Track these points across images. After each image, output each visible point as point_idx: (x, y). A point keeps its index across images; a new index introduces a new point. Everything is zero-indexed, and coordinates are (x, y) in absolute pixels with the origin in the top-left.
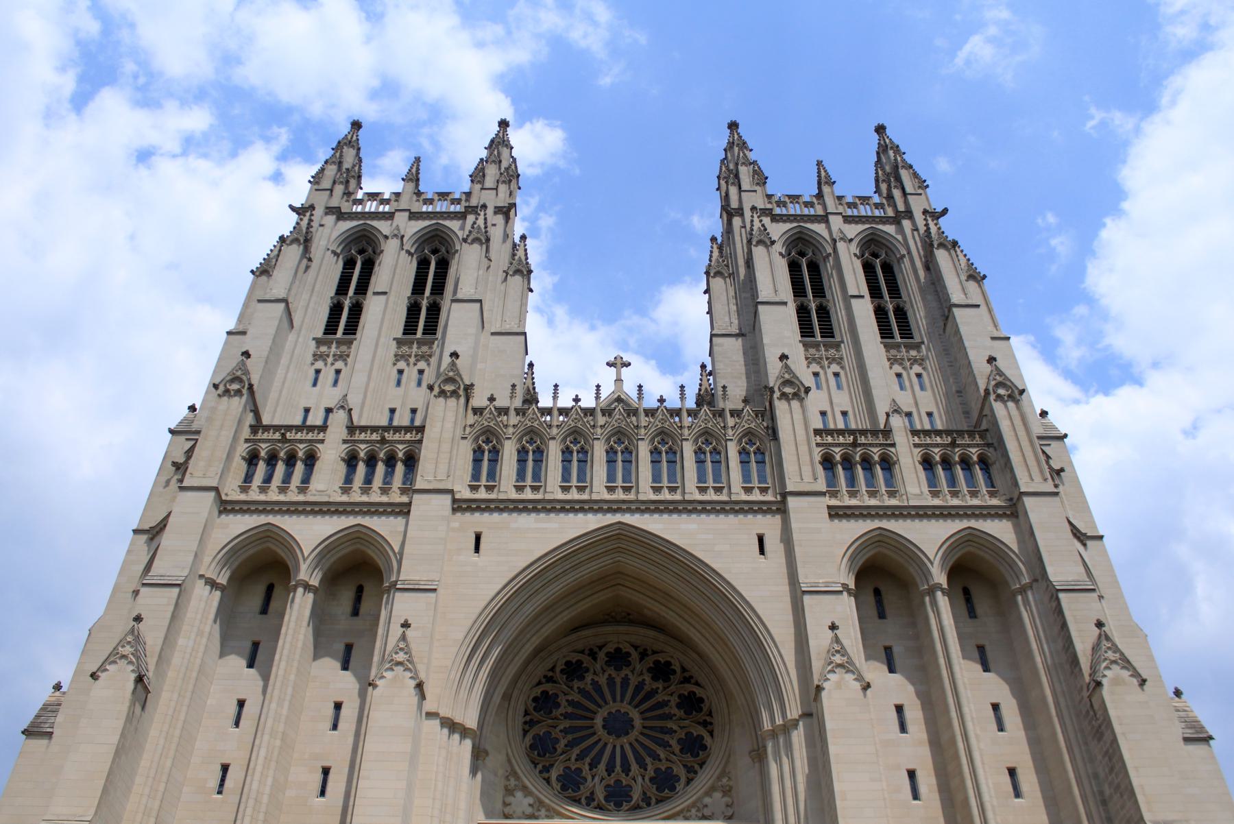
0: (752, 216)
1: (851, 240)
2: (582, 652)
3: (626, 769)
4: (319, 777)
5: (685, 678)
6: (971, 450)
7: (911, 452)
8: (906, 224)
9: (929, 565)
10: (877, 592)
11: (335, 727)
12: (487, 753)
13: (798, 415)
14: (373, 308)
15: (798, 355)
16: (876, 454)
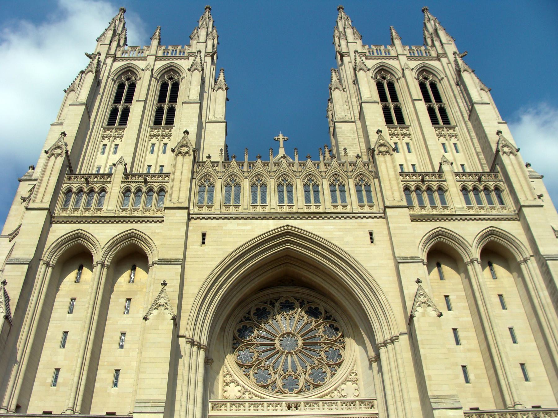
0: (355, 56)
1: (412, 69)
3: (295, 369)
5: (327, 316)
6: (490, 183)
7: (456, 185)
8: (444, 60)
9: (470, 247)
11: (121, 347)
12: (212, 360)
13: (389, 164)
14: (136, 109)
15: (386, 131)
16: (435, 185)
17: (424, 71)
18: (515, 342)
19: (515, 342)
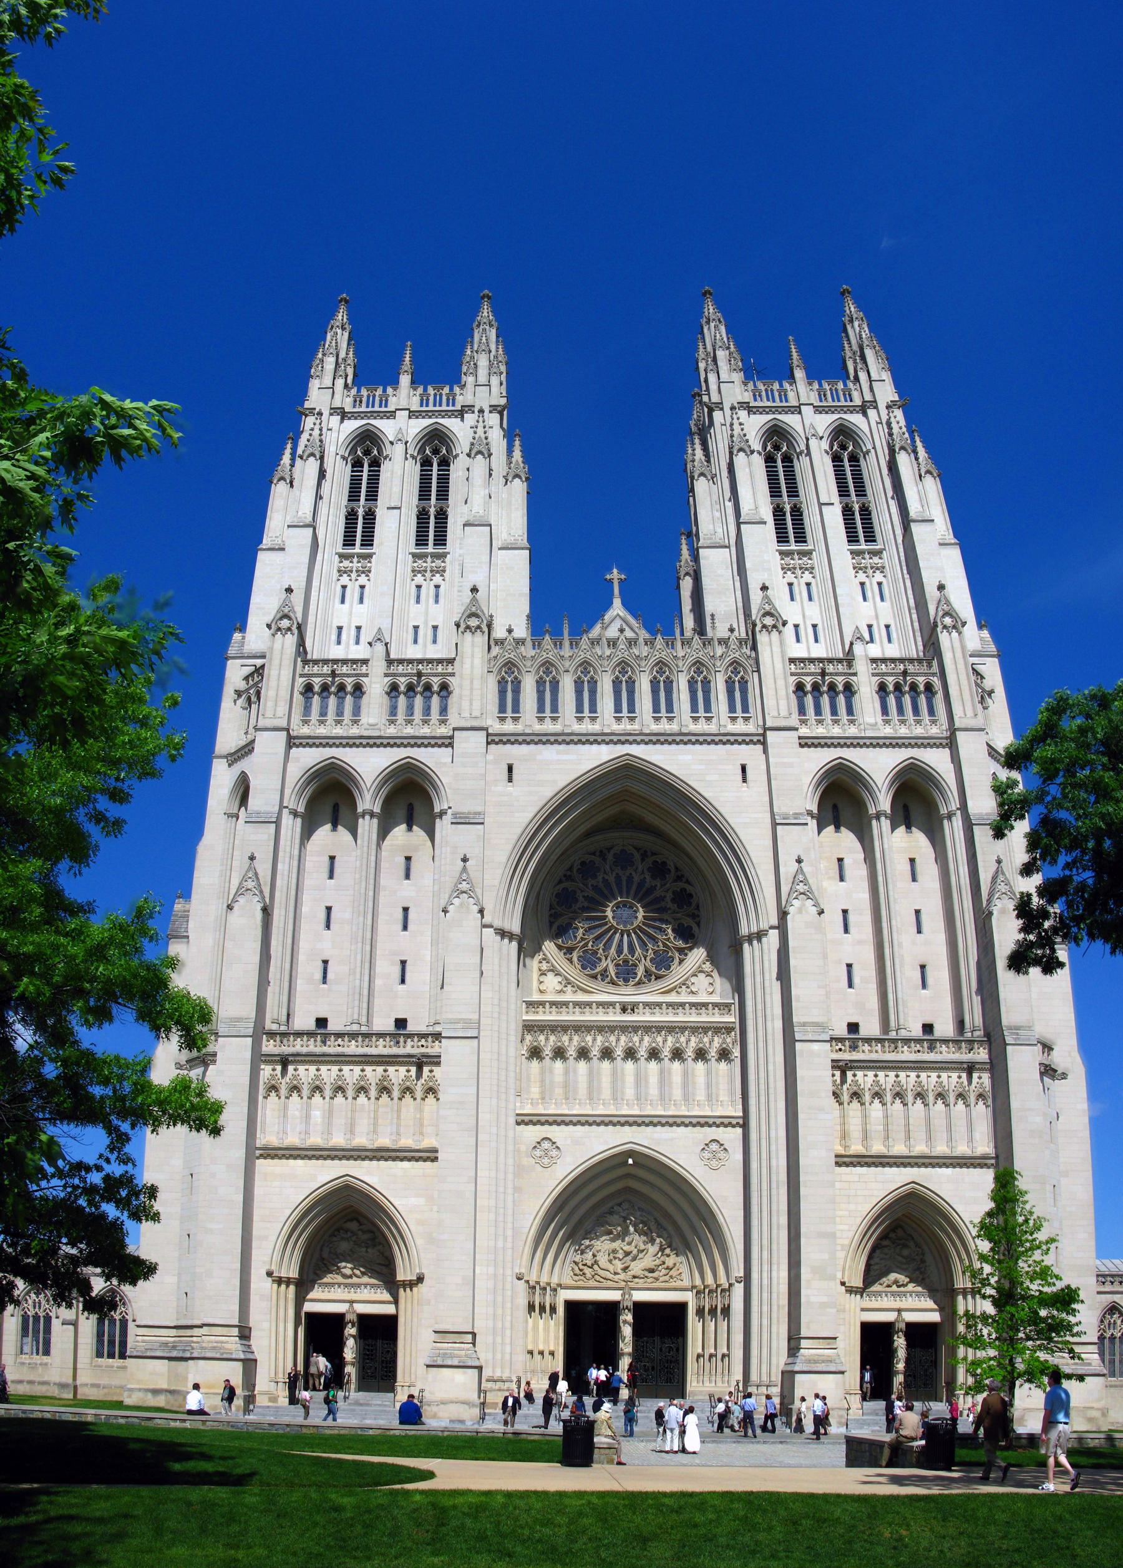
2: (594, 854)
4: (398, 968)
10: (835, 807)
13: (776, 649)
16: (840, 681)
18: (919, 932)
19: (919, 932)
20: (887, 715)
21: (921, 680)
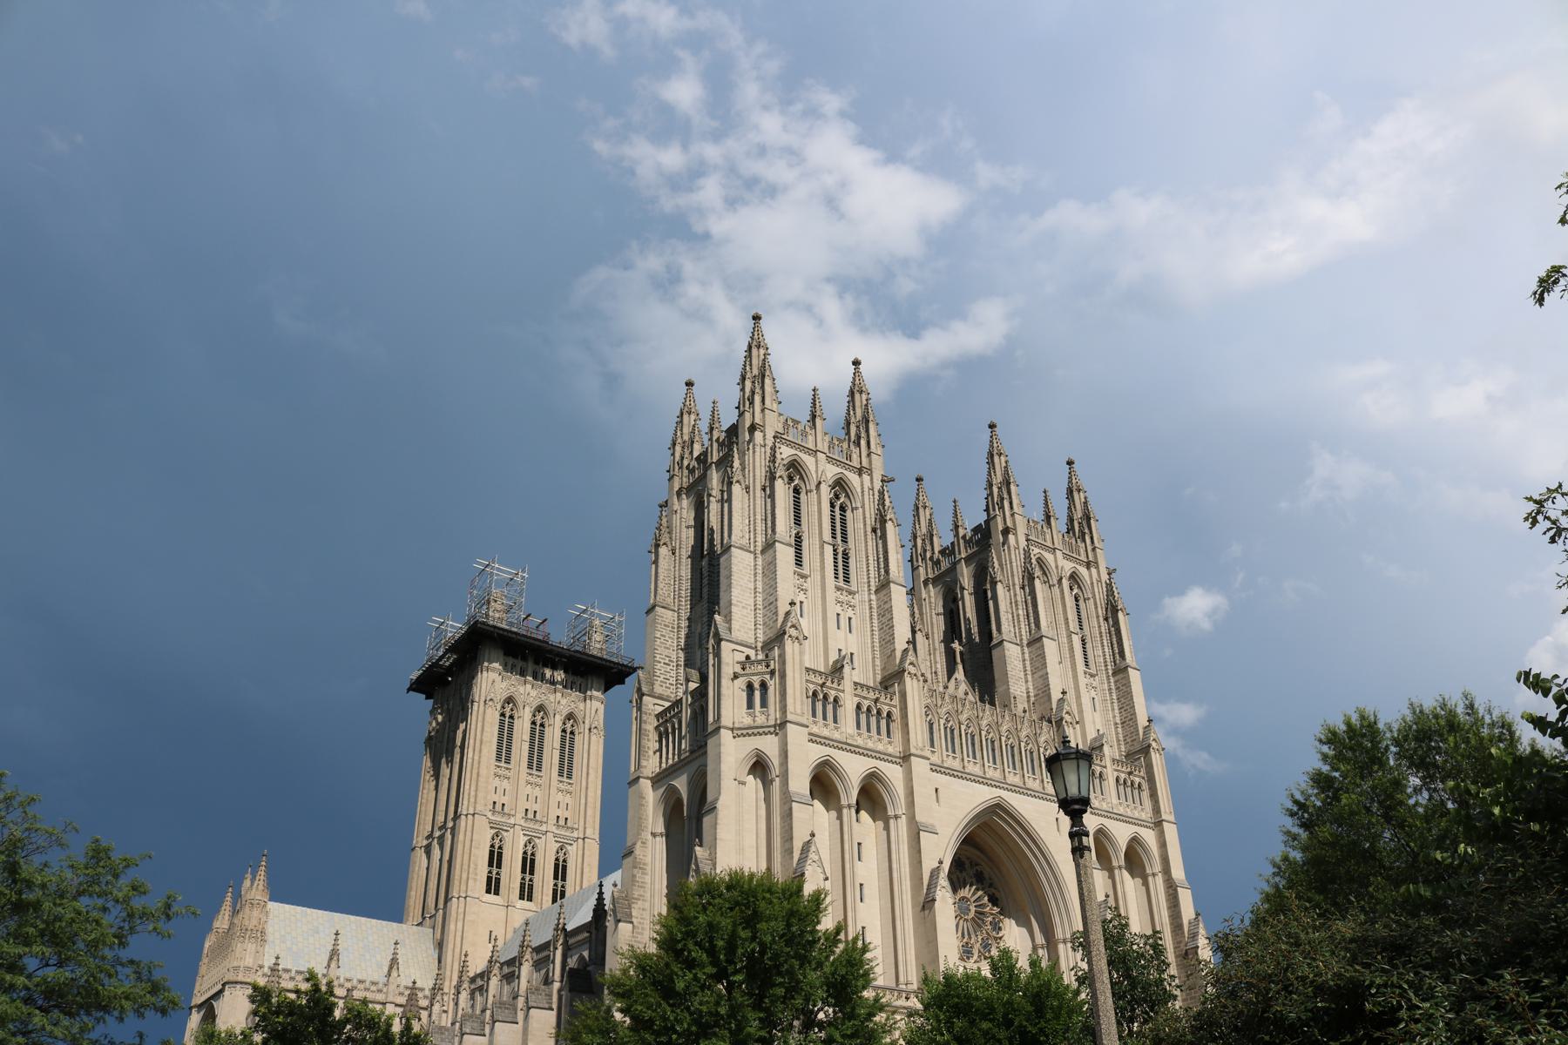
8: (866, 478)
17: (840, 485)
20: (933, 747)
21: (885, 709)
